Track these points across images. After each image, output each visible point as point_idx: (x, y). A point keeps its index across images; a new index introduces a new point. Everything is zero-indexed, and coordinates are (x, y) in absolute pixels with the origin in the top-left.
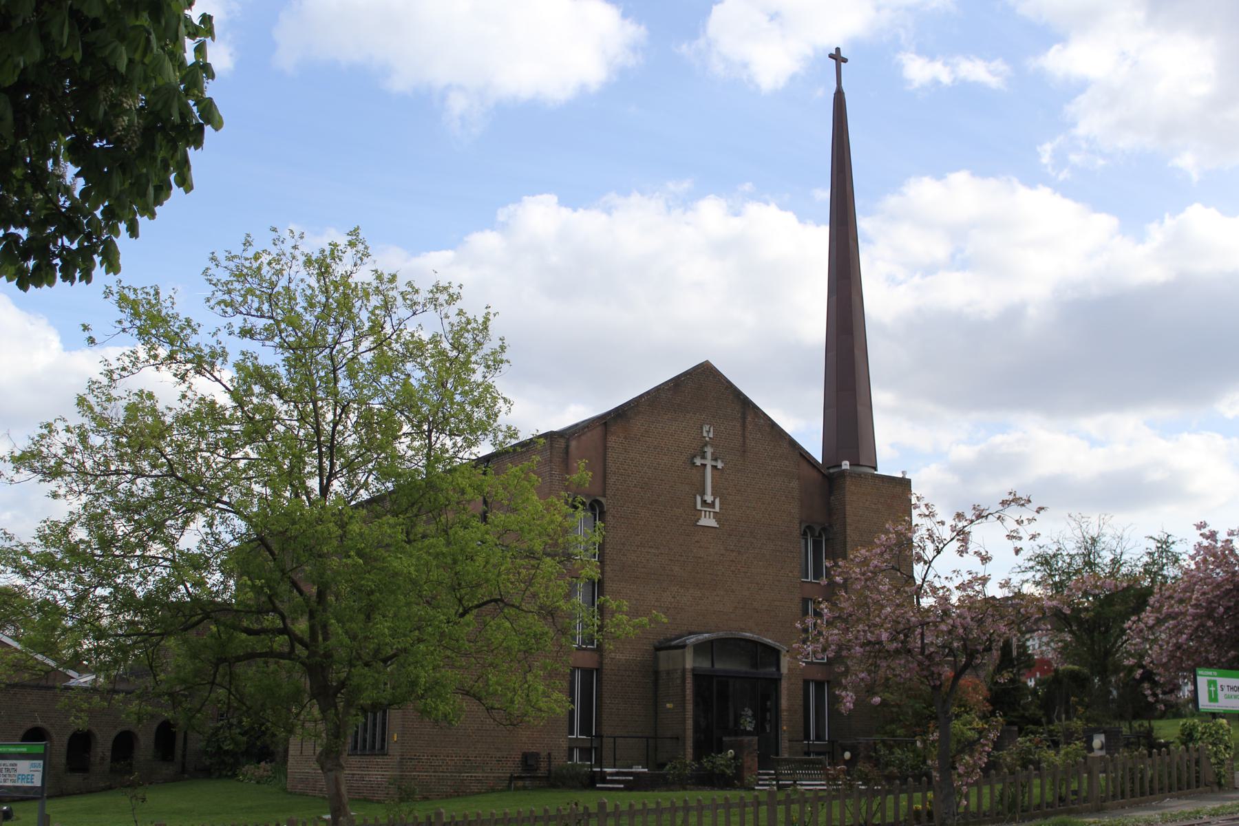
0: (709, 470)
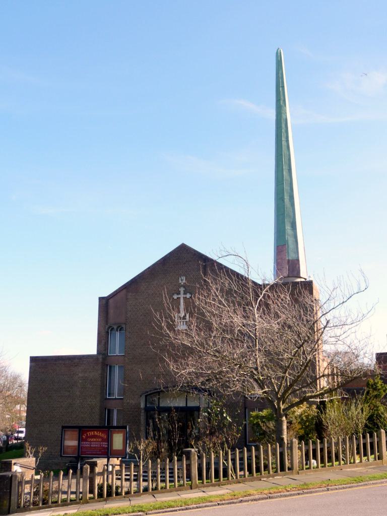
0: (182, 301)
